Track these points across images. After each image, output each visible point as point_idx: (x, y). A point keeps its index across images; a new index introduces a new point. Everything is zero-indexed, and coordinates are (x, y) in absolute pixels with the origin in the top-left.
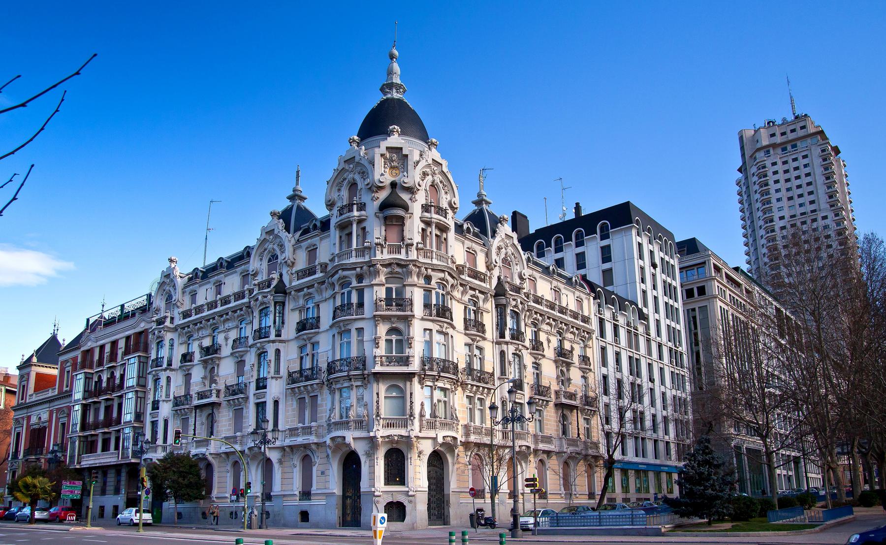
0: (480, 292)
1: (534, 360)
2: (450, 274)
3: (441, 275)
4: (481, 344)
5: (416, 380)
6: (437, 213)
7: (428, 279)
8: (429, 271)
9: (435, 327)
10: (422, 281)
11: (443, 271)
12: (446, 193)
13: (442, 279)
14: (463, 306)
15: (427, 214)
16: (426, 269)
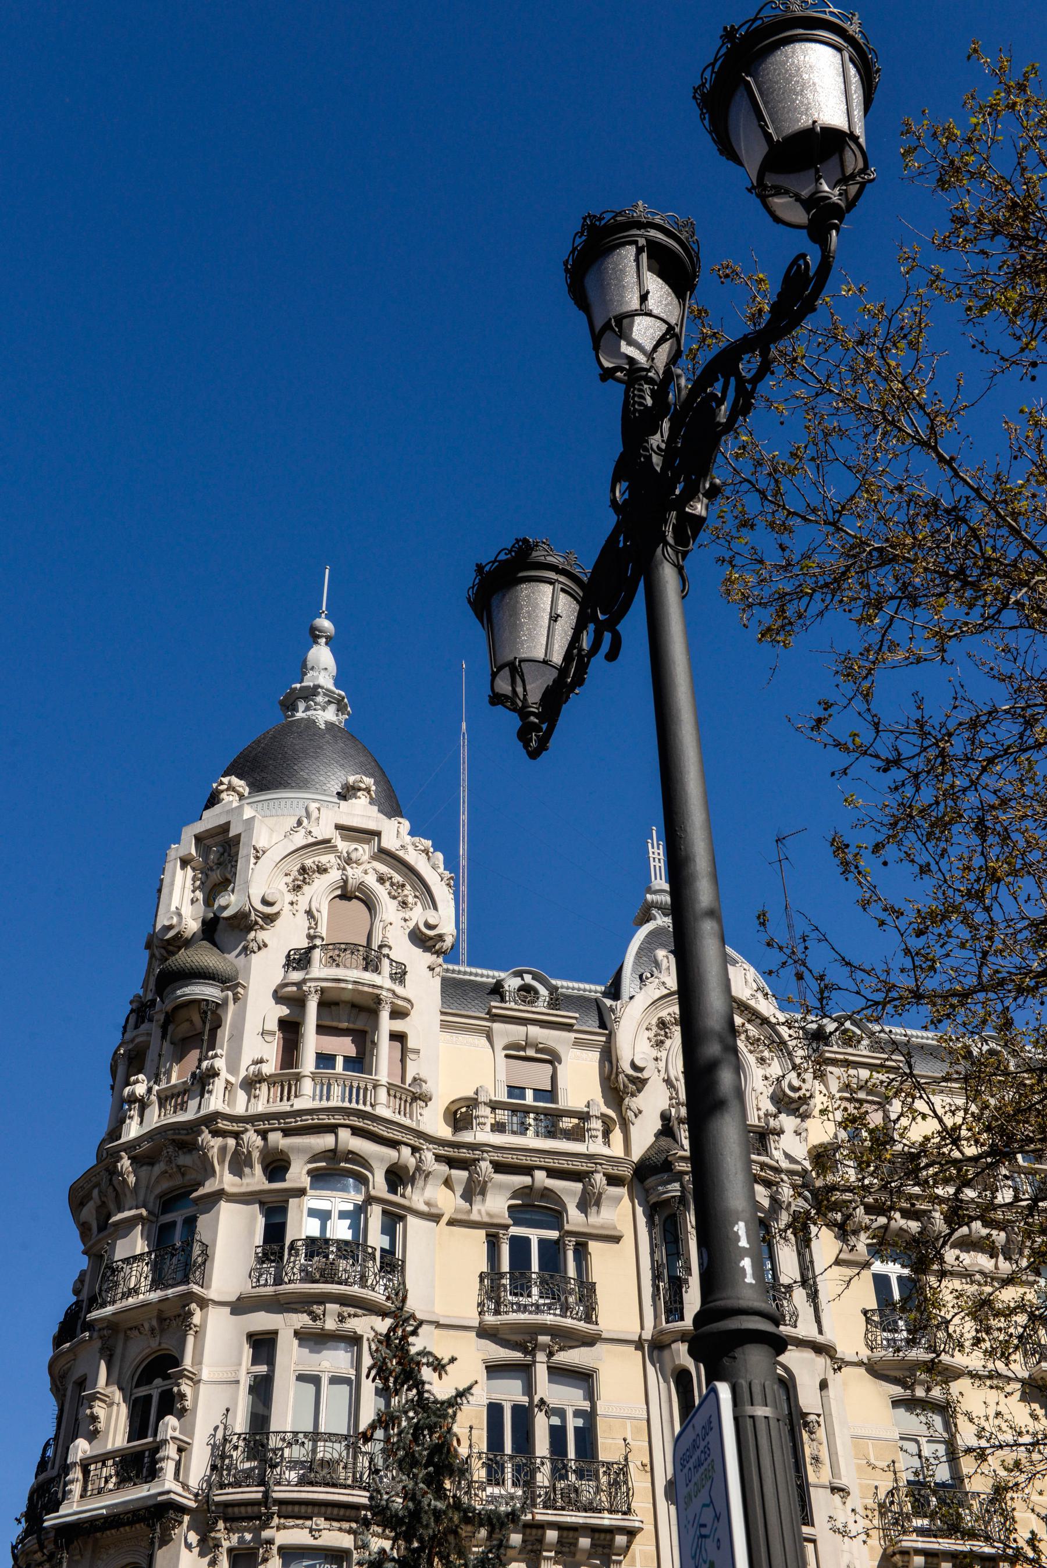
0: (552, 1173)
1: (897, 1391)
2: (356, 1132)
3: (327, 1141)
4: (574, 1357)
5: (185, 1533)
6: (333, 961)
7: (276, 1166)
8: (276, 1138)
9: (285, 1325)
10: (256, 1179)
11: (332, 1129)
12: (404, 904)
13: (332, 1155)
14: (480, 1235)
15: (296, 976)
16: (264, 1134)
